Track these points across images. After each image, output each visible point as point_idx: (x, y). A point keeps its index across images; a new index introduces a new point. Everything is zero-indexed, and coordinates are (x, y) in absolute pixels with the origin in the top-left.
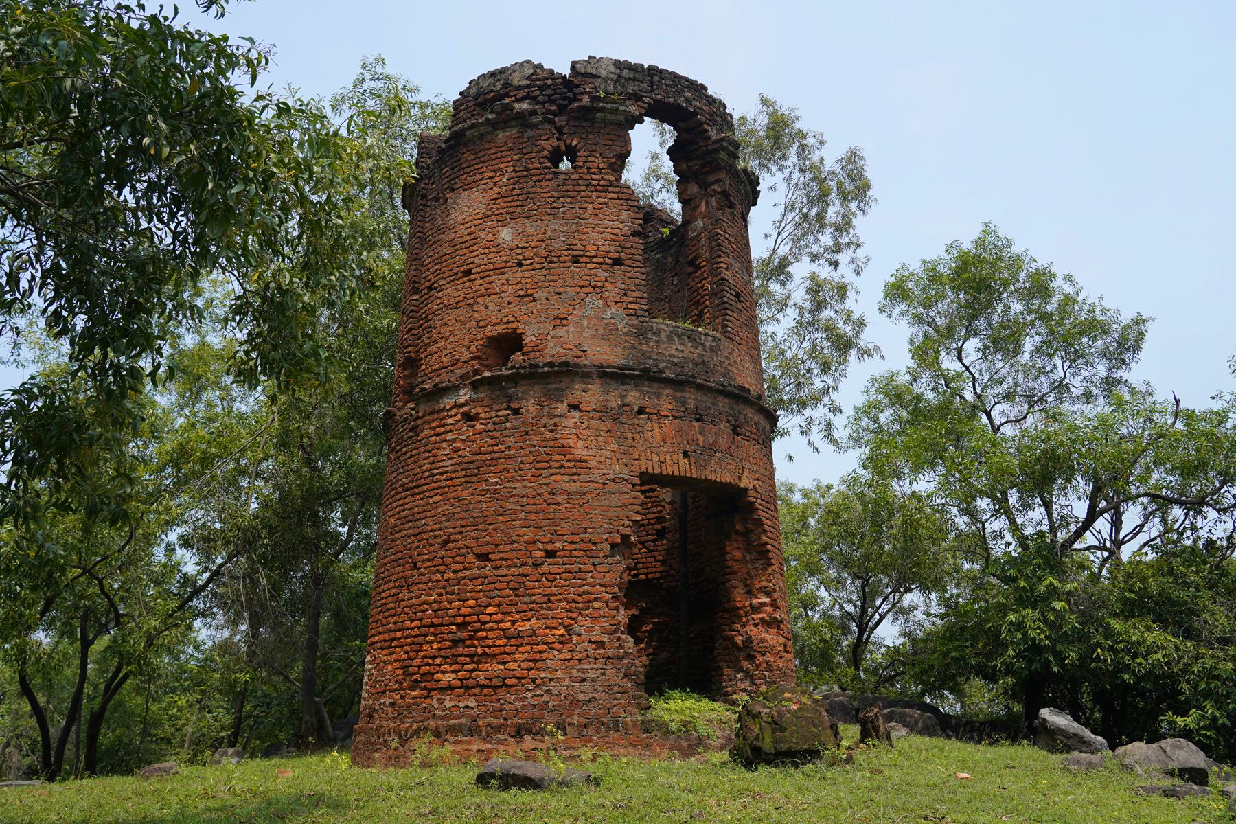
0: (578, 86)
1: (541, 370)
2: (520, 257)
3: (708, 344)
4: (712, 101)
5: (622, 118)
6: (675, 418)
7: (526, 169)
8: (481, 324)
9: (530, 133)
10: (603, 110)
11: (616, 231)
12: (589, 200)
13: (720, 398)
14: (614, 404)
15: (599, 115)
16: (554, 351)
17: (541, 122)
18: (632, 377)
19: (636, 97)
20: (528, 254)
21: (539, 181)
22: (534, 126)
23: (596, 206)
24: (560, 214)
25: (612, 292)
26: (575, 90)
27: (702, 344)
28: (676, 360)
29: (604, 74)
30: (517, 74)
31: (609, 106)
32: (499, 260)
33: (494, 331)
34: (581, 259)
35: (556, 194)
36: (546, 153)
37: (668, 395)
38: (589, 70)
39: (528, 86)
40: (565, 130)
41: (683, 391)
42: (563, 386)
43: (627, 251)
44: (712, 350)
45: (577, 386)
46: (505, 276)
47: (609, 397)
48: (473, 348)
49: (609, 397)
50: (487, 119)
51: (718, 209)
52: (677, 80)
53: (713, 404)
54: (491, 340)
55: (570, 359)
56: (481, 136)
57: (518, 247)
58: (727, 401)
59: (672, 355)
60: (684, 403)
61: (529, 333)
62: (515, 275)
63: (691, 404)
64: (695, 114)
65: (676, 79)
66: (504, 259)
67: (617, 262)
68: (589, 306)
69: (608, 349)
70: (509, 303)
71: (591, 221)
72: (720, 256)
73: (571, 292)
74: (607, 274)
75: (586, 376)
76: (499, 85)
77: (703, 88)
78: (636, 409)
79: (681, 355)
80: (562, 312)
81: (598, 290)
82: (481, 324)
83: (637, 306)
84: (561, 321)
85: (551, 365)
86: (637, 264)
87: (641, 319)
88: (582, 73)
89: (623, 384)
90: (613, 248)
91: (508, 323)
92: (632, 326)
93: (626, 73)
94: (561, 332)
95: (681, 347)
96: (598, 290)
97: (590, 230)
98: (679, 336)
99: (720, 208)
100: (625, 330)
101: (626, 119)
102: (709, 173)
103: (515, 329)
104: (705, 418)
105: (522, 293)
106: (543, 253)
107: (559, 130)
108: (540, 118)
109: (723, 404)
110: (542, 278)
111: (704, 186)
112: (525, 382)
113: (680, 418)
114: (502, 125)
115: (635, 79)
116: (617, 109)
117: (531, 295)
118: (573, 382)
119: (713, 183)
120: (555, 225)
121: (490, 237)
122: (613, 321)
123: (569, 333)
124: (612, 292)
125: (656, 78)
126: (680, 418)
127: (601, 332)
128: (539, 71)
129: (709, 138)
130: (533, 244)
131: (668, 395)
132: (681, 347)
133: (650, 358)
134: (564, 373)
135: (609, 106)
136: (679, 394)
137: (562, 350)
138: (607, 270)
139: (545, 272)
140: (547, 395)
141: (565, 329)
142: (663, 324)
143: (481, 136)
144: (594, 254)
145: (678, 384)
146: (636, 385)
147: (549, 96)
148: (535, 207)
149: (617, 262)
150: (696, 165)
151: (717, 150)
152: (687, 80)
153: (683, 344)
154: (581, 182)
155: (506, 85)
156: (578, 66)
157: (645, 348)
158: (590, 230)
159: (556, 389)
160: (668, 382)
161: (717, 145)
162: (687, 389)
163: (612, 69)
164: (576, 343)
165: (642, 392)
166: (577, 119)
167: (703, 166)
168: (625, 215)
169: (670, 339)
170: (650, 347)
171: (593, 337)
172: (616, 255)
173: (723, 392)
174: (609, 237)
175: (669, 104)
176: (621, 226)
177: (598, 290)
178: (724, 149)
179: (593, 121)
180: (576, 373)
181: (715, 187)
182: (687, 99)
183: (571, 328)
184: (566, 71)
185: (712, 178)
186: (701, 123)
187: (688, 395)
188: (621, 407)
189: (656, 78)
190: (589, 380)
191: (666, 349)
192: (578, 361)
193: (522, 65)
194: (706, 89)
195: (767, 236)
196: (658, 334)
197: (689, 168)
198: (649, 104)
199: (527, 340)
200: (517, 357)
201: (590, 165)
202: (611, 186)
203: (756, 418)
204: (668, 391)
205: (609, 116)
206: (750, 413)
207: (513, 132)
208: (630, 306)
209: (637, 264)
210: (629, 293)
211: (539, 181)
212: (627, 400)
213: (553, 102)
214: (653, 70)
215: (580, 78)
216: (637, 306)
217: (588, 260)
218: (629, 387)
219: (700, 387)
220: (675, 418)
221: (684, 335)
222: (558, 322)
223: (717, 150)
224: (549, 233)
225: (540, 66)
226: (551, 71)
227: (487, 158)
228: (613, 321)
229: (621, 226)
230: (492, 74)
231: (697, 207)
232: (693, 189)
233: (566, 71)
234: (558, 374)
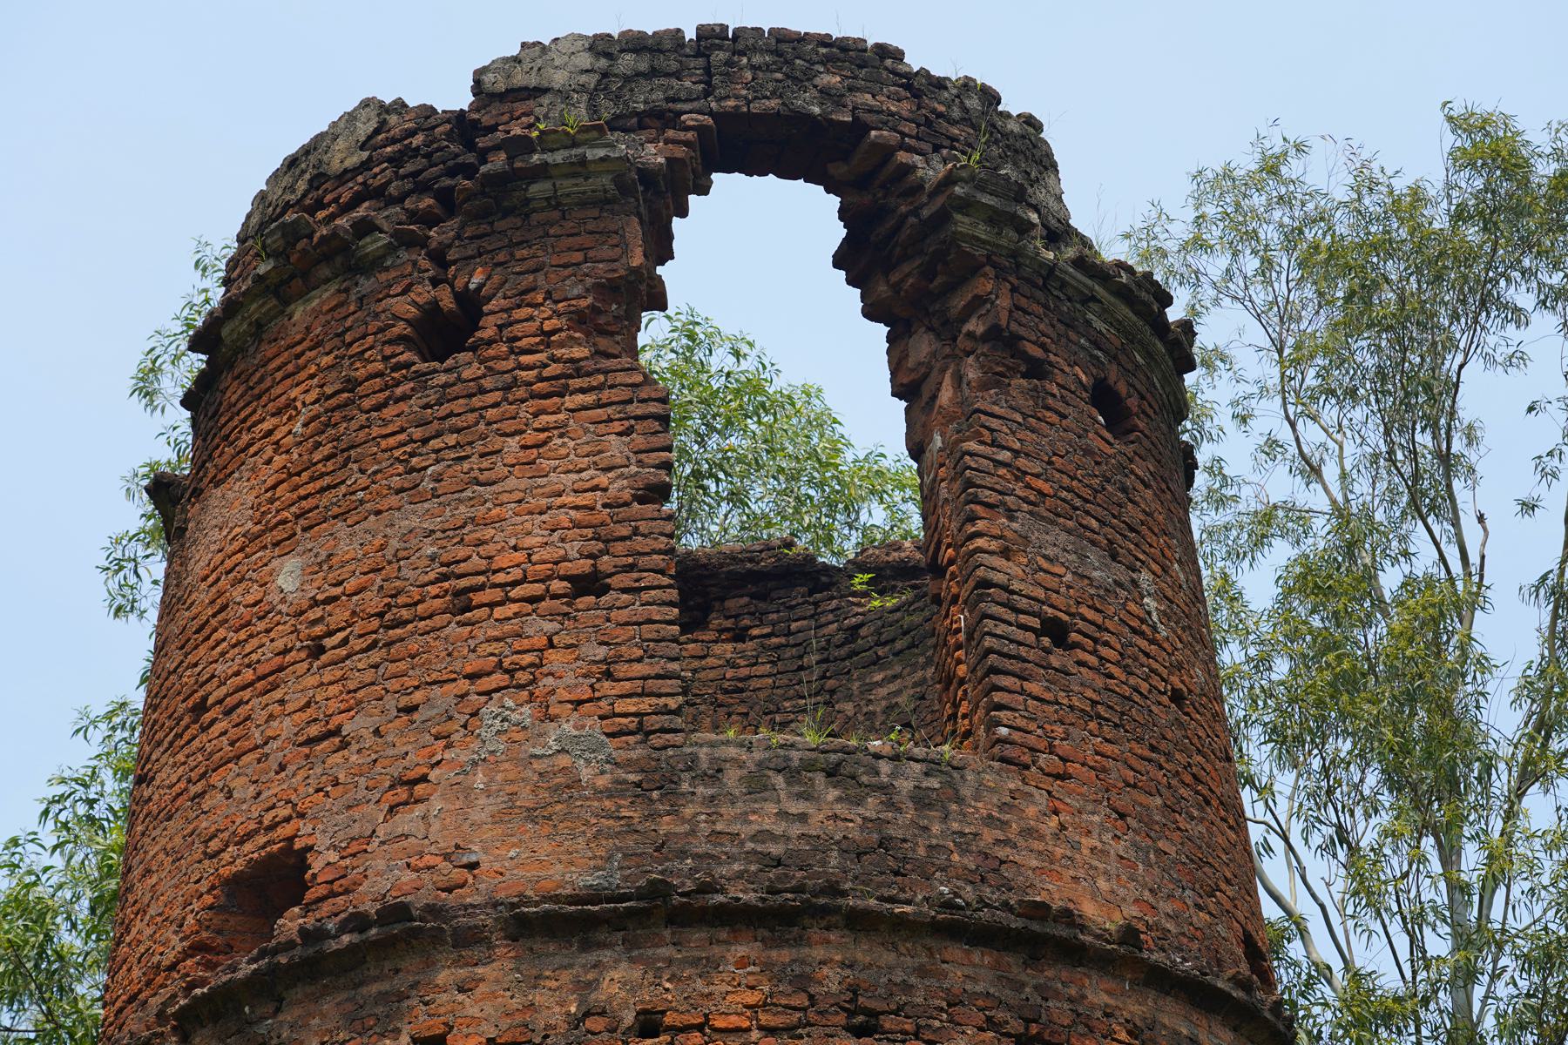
0: (493, 129)
1: (334, 945)
2: (318, 630)
3: (905, 785)
4: (923, 86)
5: (605, 180)
6: (770, 1031)
7: (351, 385)
8: (214, 845)
9: (366, 285)
10: (543, 171)
11: (585, 499)
12: (508, 426)
13: (955, 951)
14: (556, 1016)
15: (538, 189)
16: (384, 879)
17: (390, 249)
18: (615, 922)
19: (660, 119)
20: (339, 615)
21: (378, 408)
22: (373, 265)
23: (531, 437)
24: (428, 485)
25: (565, 674)
26: (482, 142)
27: (886, 789)
28: (776, 849)
29: (559, 79)
30: (341, 144)
31: (559, 157)
32: (266, 653)
33: (236, 860)
34: (478, 598)
35: (418, 433)
36: (400, 328)
37: (742, 963)
38: (520, 79)
39: (365, 166)
40: (452, 255)
41: (799, 941)
42: (400, 983)
43: (619, 547)
44: (922, 800)
45: (443, 977)
46: (277, 694)
47: (538, 997)
48: (190, 920)
49: (538, 997)
50: (259, 279)
51: (984, 386)
52: (788, 50)
53: (922, 972)
54: (234, 885)
55: (419, 901)
56: (259, 327)
57: (315, 603)
58: (982, 958)
59: (762, 836)
60: (802, 982)
61: (322, 842)
62: (301, 684)
63: (832, 981)
64: (859, 128)
65: (785, 44)
66: (279, 645)
67: (589, 584)
68: (489, 725)
69: (545, 847)
70: (282, 768)
71: (512, 483)
72: (972, 519)
73: (443, 697)
74: (550, 627)
75: (469, 940)
76: (302, 186)
77: (888, 54)
78: (629, 1018)
79: (796, 830)
80: (415, 761)
81: (522, 677)
82: (214, 845)
83: (645, 704)
84: (411, 785)
85: (358, 922)
86: (650, 578)
87: (656, 740)
88: (500, 91)
89: (586, 946)
90: (573, 549)
91: (273, 826)
92: (628, 765)
93: (629, 58)
94: (407, 821)
95: (796, 807)
96: (522, 677)
97: (507, 512)
98: (792, 774)
99: (994, 380)
100: (602, 782)
101: (619, 181)
102: (951, 288)
103: (290, 839)
104: (888, 1022)
105: (314, 730)
106: (373, 602)
107: (439, 258)
108: (384, 239)
109: (966, 969)
110: (369, 676)
111: (947, 330)
112: (298, 992)
113: (790, 1030)
114: (298, 283)
115: (654, 73)
116: (583, 161)
117: (336, 732)
118: (430, 965)
119: (965, 317)
120: (412, 519)
121: (255, 593)
122: (564, 761)
123: (433, 821)
124: (565, 674)
125: (720, 56)
126: (790, 1030)
127: (526, 798)
128: (393, 119)
129: (920, 187)
130: (351, 585)
131: (742, 963)
132: (796, 807)
133: (682, 854)
134: (407, 935)
135: (559, 157)
136: (783, 955)
137: (408, 877)
138: (552, 615)
139: (375, 655)
140: (355, 1020)
141: (419, 810)
142: (729, 745)
143: (259, 327)
144: (516, 574)
145: (777, 919)
146: (631, 944)
147: (415, 174)
148: (364, 481)
149: (589, 584)
150: (907, 273)
151: (942, 217)
152: (824, 41)
153: (805, 796)
154: (487, 383)
155: (319, 179)
156: (488, 78)
157: (666, 825)
158: (507, 512)
159: (383, 997)
160: (735, 918)
161: (940, 200)
162: (815, 934)
163: (585, 60)
164: (446, 844)
165: (649, 963)
166: (482, 215)
167: (928, 273)
168: (616, 447)
169: (757, 786)
170: (687, 817)
171: (497, 819)
172: (585, 566)
173: (955, 927)
174: (563, 517)
175: (763, 117)
176: (603, 480)
177: (521, 677)
178: (966, 205)
179: (524, 210)
180: (437, 937)
181: (975, 326)
182: (825, 93)
183: (436, 804)
184: (458, 98)
185: (959, 302)
186: (887, 152)
187: (819, 953)
188: (576, 1022)
189: (720, 56)
190: (476, 953)
191: (743, 818)
192: (450, 899)
193: (350, 117)
194: (898, 55)
195: (1528, 507)
196: (715, 774)
197: (896, 287)
198: (700, 129)
199: (316, 864)
200: (291, 923)
201: (517, 330)
202: (579, 373)
203: (1136, 1007)
204: (741, 950)
205: (566, 185)
206: (1098, 993)
207: (324, 297)
208: (620, 707)
209: (650, 578)
210: (621, 669)
211: (378, 408)
212: (598, 997)
213: (422, 188)
214: (711, 36)
215: (496, 108)
216: (645, 704)
217: (497, 594)
218: (606, 956)
219: (860, 923)
220: (770, 1031)
221: (809, 766)
222: (402, 793)
223: (942, 217)
224: (394, 543)
225: (400, 106)
226: (428, 111)
227: (268, 382)
228: (564, 761)
229: (603, 480)
230: (292, 163)
231: (934, 397)
232: (922, 346)
233: (458, 98)
234: (385, 946)
